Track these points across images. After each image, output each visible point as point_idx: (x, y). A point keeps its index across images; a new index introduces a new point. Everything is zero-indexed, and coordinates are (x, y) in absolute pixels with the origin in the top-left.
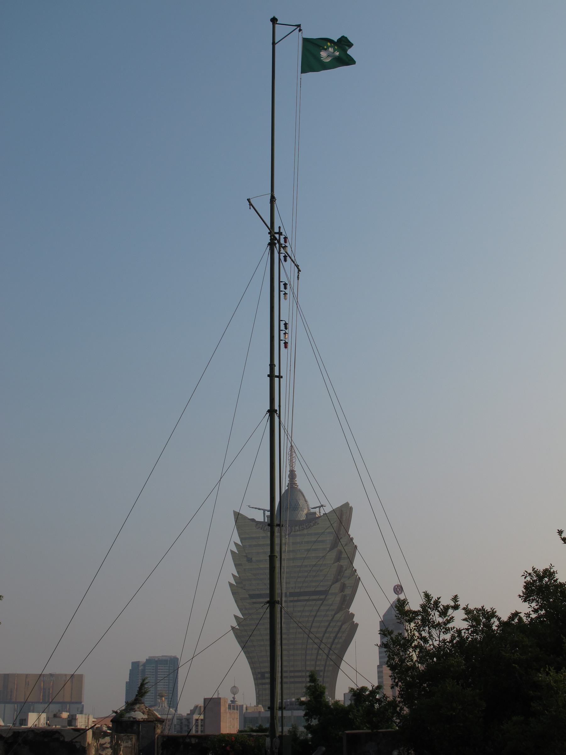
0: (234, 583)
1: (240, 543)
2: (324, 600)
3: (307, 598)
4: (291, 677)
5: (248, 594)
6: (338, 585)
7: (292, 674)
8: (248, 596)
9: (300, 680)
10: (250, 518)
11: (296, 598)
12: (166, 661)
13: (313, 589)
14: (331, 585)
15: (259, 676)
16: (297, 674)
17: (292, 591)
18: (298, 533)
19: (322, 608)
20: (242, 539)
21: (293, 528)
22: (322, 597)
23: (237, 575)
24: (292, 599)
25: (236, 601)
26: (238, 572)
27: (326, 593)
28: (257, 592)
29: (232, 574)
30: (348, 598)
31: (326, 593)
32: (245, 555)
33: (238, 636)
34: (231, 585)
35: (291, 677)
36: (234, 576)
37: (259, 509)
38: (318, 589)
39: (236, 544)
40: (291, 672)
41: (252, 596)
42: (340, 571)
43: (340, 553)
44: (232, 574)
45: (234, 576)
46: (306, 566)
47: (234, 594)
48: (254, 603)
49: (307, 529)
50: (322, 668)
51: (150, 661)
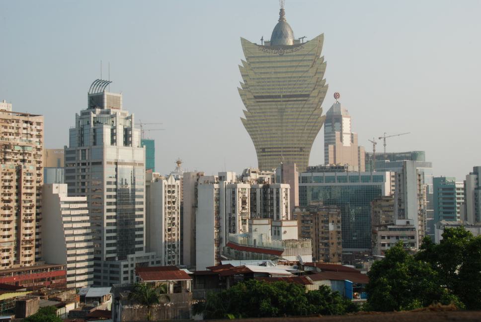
0: (241, 88)
1: (245, 60)
3: (295, 99)
5: (254, 96)
8: (253, 97)
10: (253, 42)
11: (287, 99)
13: (299, 93)
15: (261, 150)
17: (284, 94)
19: (305, 106)
22: (306, 99)
23: (243, 83)
26: (244, 81)
27: (308, 96)
34: (239, 89)
36: (241, 83)
38: (302, 93)
39: (243, 61)
40: (284, 148)
41: (256, 97)
45: (241, 83)
46: (295, 77)
47: (241, 95)
48: (258, 102)
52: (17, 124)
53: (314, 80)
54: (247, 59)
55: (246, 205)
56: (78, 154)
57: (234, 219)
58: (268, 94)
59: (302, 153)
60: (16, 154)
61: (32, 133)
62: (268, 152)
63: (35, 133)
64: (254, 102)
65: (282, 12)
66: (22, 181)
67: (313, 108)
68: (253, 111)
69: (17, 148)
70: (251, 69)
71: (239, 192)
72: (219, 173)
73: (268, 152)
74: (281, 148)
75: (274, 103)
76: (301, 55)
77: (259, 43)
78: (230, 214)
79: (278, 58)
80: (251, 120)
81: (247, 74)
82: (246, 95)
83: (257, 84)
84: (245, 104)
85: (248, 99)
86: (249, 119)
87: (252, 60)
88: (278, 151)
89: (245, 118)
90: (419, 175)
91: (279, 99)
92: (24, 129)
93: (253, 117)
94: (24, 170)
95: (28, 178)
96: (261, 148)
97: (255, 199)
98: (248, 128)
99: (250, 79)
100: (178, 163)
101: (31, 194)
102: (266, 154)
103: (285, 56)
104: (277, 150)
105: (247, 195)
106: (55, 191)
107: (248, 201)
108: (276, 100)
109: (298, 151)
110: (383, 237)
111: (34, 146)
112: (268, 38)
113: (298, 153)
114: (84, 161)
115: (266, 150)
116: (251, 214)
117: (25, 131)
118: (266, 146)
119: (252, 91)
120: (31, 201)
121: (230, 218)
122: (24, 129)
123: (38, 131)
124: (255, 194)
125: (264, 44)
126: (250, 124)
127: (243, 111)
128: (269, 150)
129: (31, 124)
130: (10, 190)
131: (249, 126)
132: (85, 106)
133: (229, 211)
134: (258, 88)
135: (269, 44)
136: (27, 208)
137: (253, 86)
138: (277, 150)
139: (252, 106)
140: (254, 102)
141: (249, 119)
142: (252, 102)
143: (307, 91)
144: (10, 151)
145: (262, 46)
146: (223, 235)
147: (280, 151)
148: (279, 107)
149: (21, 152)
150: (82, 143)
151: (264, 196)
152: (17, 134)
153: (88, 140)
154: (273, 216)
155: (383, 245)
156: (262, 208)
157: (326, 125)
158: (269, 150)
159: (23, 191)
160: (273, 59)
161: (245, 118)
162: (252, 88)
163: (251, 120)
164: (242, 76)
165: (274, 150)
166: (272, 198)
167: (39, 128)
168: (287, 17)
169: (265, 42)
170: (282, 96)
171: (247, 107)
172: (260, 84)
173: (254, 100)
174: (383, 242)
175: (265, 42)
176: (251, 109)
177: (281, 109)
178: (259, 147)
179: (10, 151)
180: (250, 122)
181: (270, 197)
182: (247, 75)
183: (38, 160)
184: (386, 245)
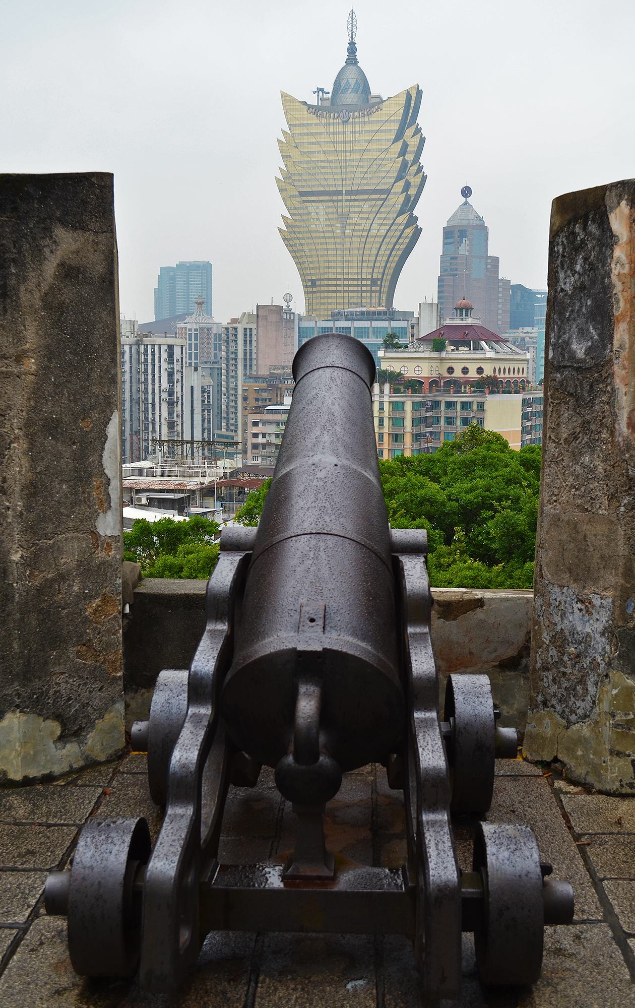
2: (385, 200)
3: (365, 197)
4: (344, 285)
6: (401, 184)
7: (346, 282)
9: (355, 289)
11: (353, 197)
12: (199, 266)
14: (395, 183)
15: (310, 283)
16: (351, 282)
17: (349, 188)
18: (358, 120)
19: (382, 209)
20: (291, 126)
21: (352, 114)
22: (384, 196)
24: (348, 197)
25: (284, 199)
26: (286, 166)
27: (388, 192)
28: (309, 189)
29: (279, 168)
30: (412, 199)
31: (388, 192)
32: (294, 145)
33: (285, 239)
34: (278, 180)
35: (344, 285)
39: (283, 132)
41: (302, 194)
42: (404, 166)
43: (405, 146)
44: (279, 168)
49: (368, 115)
50: (380, 277)
51: (181, 266)
53: (398, 165)
58: (322, 189)
59: (374, 289)
62: (321, 286)
65: (352, 49)
67: (394, 212)
70: (296, 147)
73: (321, 286)
74: (340, 279)
75: (330, 204)
76: (377, 122)
77: (313, 101)
80: (295, 233)
85: (291, 197)
86: (290, 230)
87: (297, 131)
88: (349, 285)
90: (413, 327)
91: (340, 198)
93: (297, 226)
98: (291, 245)
102: (318, 289)
103: (352, 123)
108: (335, 198)
109: (366, 286)
110: (255, 424)
113: (369, 288)
115: (318, 283)
127: (283, 216)
128: (322, 283)
135: (328, 104)
139: (295, 208)
141: (290, 230)
142: (296, 202)
143: (385, 184)
147: (340, 285)
148: (340, 210)
155: (255, 435)
157: (446, 241)
158: (322, 283)
163: (295, 233)
166: (146, 360)
168: (359, 55)
170: (344, 192)
173: (298, 199)
174: (255, 430)
177: (343, 214)
180: (293, 236)
182: (289, 157)
184: (260, 436)
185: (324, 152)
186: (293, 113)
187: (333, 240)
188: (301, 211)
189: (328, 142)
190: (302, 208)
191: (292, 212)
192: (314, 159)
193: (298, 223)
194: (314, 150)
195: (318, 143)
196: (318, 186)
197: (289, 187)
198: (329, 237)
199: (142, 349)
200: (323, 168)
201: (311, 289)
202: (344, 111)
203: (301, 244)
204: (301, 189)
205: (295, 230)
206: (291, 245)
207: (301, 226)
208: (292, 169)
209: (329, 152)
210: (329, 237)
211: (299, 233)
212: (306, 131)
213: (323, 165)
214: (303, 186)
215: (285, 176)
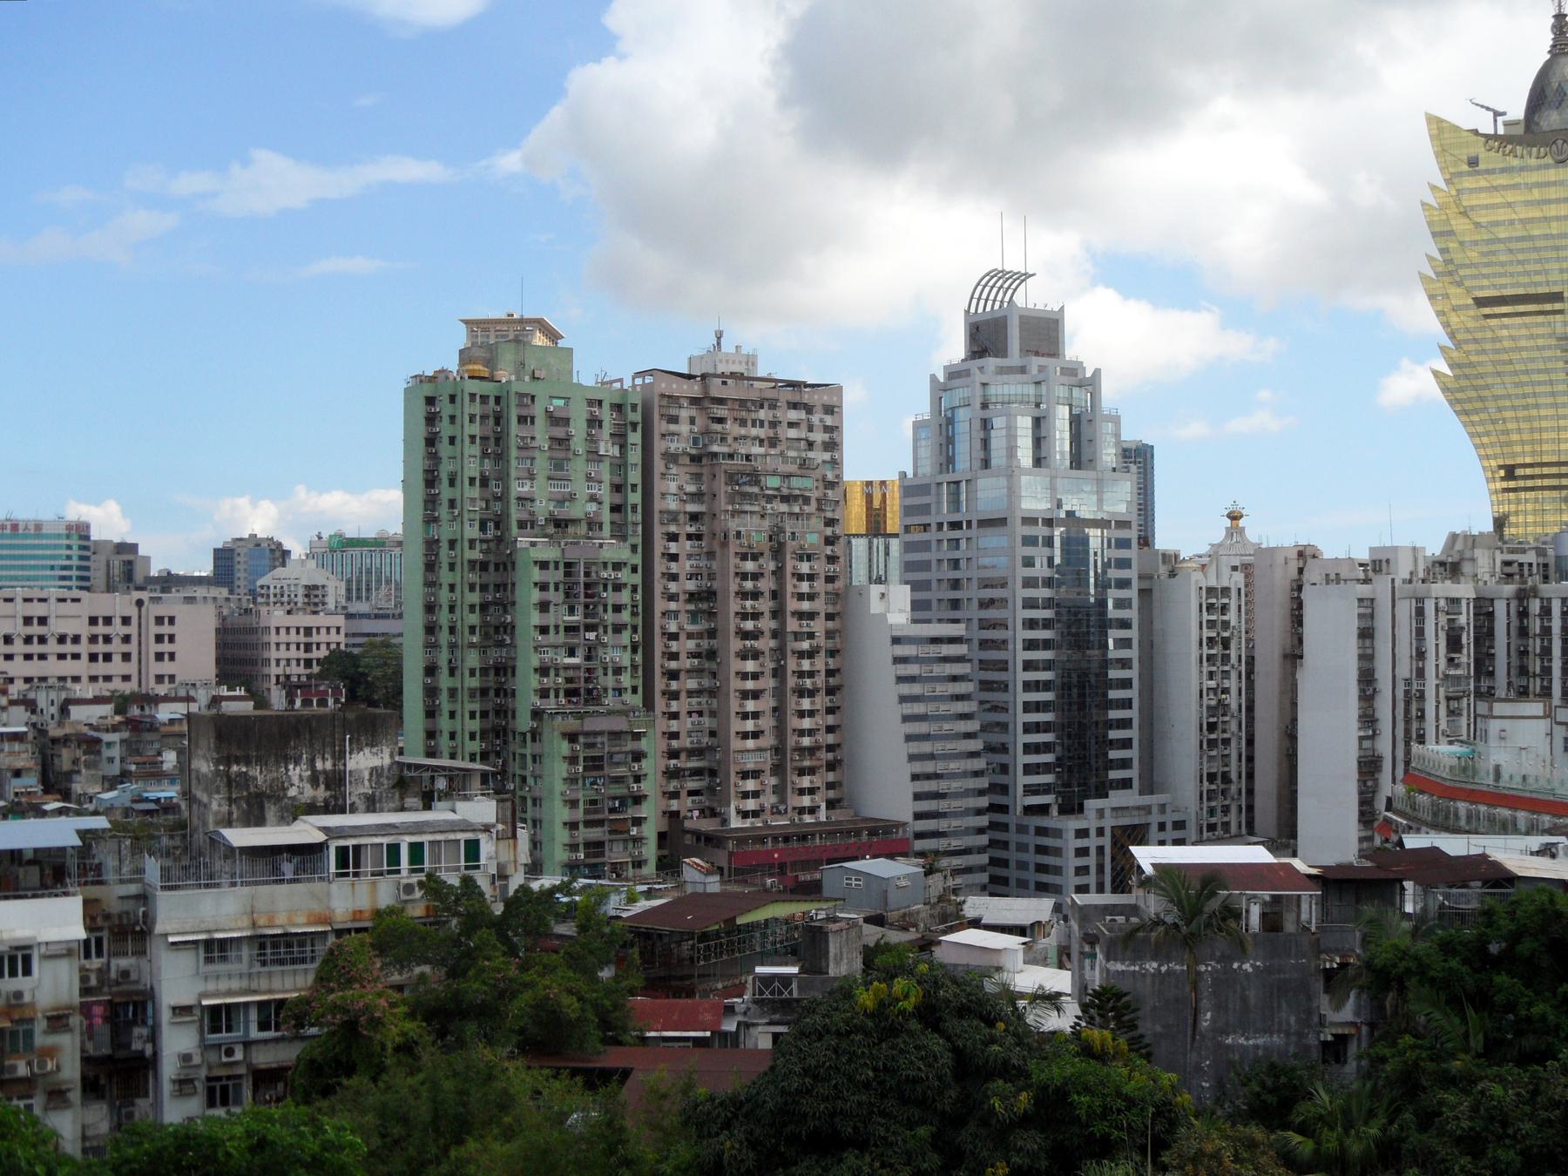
1: (1443, 185)
5: (1476, 299)
8: (1470, 301)
15: (1502, 473)
25: (1440, 314)
26: (1443, 251)
33: (1445, 389)
34: (1424, 279)
37: (1488, 109)
39: (1434, 188)
41: (1480, 302)
45: (1431, 259)
48: (1487, 316)
52: (771, 413)
54: (1448, 182)
55: (1459, 651)
56: (939, 495)
57: (1421, 696)
58: (1521, 291)
60: (770, 499)
61: (812, 436)
63: (819, 437)
64: (1473, 317)
66: (789, 576)
68: (1472, 347)
69: (773, 482)
70: (1464, 214)
71: (1437, 610)
72: (1372, 550)
75: (1540, 319)
78: (1408, 682)
79: (1552, 171)
80: (1467, 377)
81: (1449, 228)
82: (1447, 296)
83: (1485, 260)
84: (1446, 325)
85: (1455, 309)
89: (1449, 372)
92: (791, 425)
93: (1471, 365)
94: (791, 546)
95: (805, 568)
96: (1500, 467)
97: (1491, 633)
98: (1458, 401)
99: (1462, 243)
100: (1234, 517)
101: (811, 616)
102: (1521, 483)
104: (1554, 470)
105: (1462, 620)
106: (876, 606)
107: (1467, 639)
111: (818, 474)
112: (1517, 111)
114: (956, 518)
115: (1519, 472)
116: (1477, 679)
117: (793, 433)
118: (1520, 460)
119: (1468, 283)
120: (811, 636)
121: (1407, 692)
122: (791, 425)
123: (828, 429)
124: (1491, 615)
125: (1501, 131)
126: (1461, 389)
128: (1529, 471)
129: (809, 409)
130: (756, 603)
131: (1459, 395)
132: (955, 348)
133: (1404, 670)
134: (1485, 271)
136: (801, 655)
137: (1471, 265)
138: (1554, 470)
139: (1468, 330)
140: (1475, 318)
141: (1458, 372)
142: (1467, 319)
144: (756, 490)
145: (1495, 137)
146: (1384, 746)
149: (785, 491)
150: (948, 462)
151: (1521, 622)
152: (773, 442)
153: (965, 451)
154: (1550, 688)
156: (1515, 662)
158: (1529, 471)
159: (792, 605)
160: (1534, 177)
161: (1447, 371)
162: (1468, 272)
163: (1467, 377)
164: (1434, 234)
165: (1546, 471)
166: (1547, 631)
167: (829, 421)
169: (1506, 124)
171: (1452, 336)
172: (1494, 259)
173: (1471, 313)
175: (1506, 124)
176: (1466, 342)
178: (1493, 463)
179: (756, 490)
180: (1464, 383)
181: (1542, 627)
183: (829, 515)
185: (1521, 221)
186: (1456, 152)
187: (1548, 388)
188: (1479, 335)
189: (1528, 203)
190: (1483, 329)
191: (1459, 337)
192: (1502, 236)
193: (1474, 358)
194: (1501, 218)
195: (1509, 205)
196: (1513, 285)
197: (1453, 290)
198: (1540, 383)
199: (1535, 606)
200: (1522, 251)
201: (1505, 485)
202: (1560, 142)
203: (1482, 399)
204: (1481, 294)
205: (1467, 371)
206: (1458, 401)
207: (1480, 364)
208: (1458, 257)
209: (1531, 220)
210: (1540, 383)
211: (1476, 377)
212: (1483, 183)
213: (1520, 245)
214: (1482, 288)
215: (1440, 269)
